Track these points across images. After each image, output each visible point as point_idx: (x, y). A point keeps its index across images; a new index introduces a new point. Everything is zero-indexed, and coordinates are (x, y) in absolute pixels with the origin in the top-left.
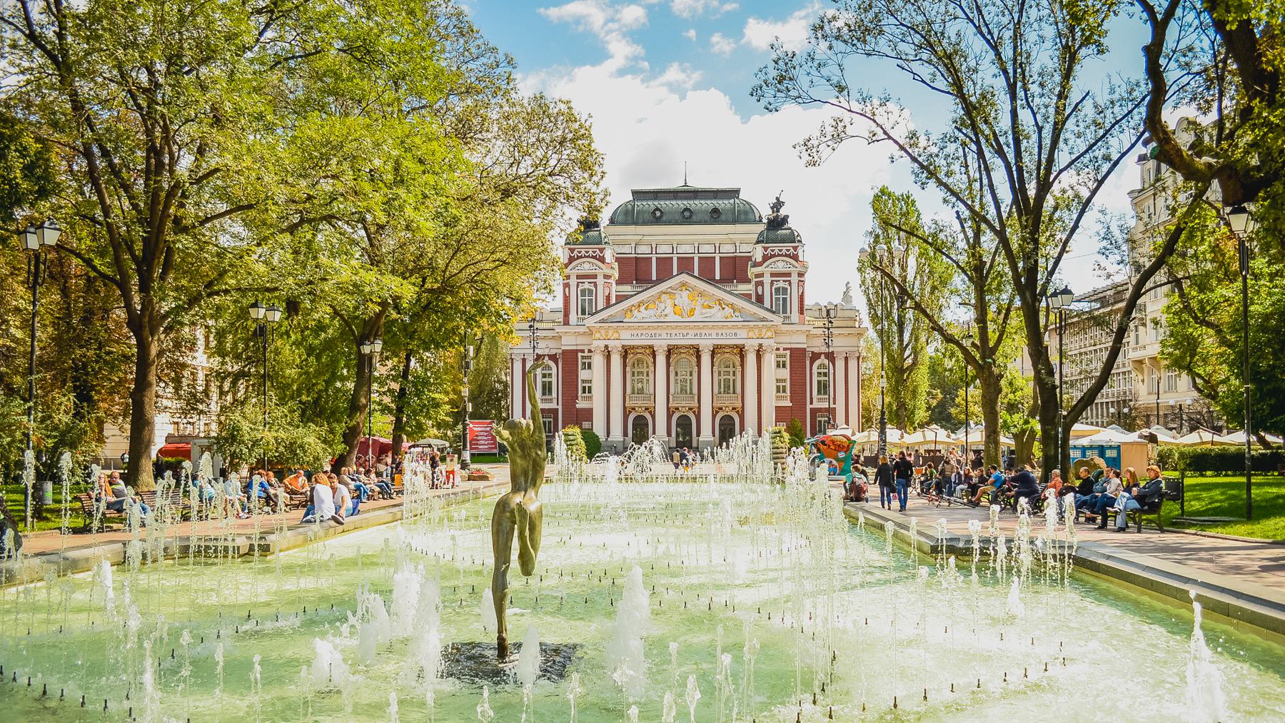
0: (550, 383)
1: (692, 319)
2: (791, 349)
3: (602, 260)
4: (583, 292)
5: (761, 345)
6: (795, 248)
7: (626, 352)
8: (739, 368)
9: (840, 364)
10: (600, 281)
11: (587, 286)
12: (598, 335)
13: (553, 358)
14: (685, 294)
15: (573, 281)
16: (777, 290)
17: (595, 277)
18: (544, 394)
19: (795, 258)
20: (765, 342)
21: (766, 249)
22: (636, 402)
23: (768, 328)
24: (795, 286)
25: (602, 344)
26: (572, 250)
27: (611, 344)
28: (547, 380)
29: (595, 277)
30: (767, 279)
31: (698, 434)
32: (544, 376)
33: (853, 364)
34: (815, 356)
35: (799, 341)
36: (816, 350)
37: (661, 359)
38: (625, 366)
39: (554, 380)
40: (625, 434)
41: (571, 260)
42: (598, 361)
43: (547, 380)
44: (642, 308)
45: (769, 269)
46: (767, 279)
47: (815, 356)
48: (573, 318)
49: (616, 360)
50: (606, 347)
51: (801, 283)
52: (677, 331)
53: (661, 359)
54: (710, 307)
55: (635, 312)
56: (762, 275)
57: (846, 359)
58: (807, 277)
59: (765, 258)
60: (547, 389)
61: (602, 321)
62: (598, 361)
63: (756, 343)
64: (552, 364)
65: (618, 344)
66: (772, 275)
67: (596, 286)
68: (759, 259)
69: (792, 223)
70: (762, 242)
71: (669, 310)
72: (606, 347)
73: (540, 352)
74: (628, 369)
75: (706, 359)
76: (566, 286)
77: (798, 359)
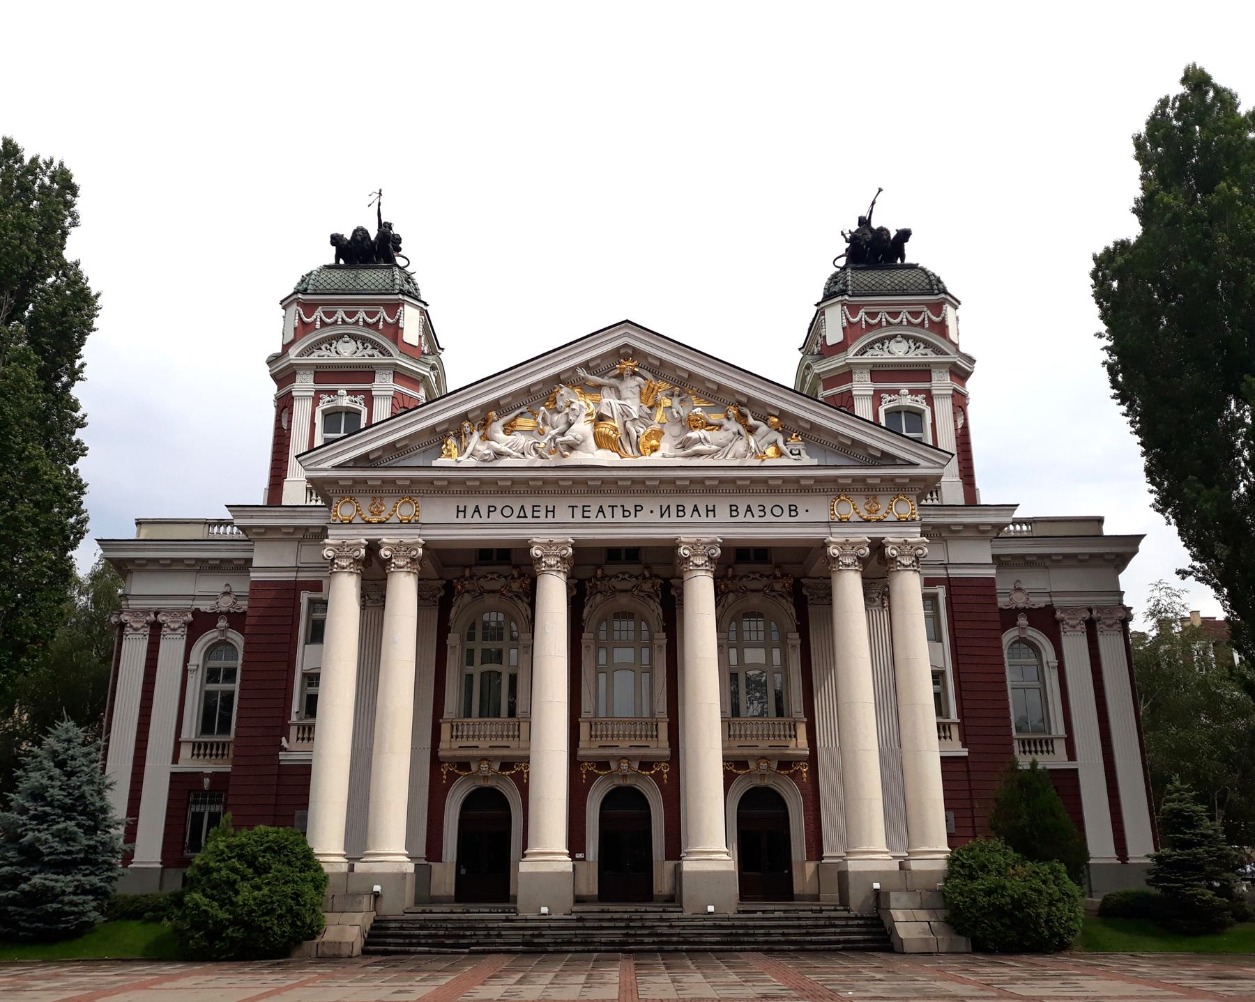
0: (228, 697)
1: (654, 459)
2: (949, 582)
3: (395, 332)
4: (332, 417)
5: (878, 546)
6: (937, 308)
7: (450, 589)
8: (795, 638)
9: (1075, 645)
10: (384, 385)
11: (345, 401)
12: (345, 511)
13: (237, 620)
14: (631, 386)
15: (304, 386)
16: (893, 414)
17: (366, 374)
18: (206, 727)
19: (941, 328)
20: (891, 536)
21: (854, 308)
22: (479, 739)
23: (897, 488)
24: (944, 408)
25: (361, 536)
26: (309, 308)
27: (388, 537)
28: (221, 687)
29: (366, 374)
30: (862, 386)
31: (675, 850)
32: (212, 676)
33: (1110, 646)
34: (1009, 618)
35: (974, 559)
36: (1002, 602)
37: (554, 594)
38: (443, 631)
39: (236, 687)
40: (434, 850)
41: (304, 328)
42: (345, 593)
43: (221, 687)
44: (497, 428)
45: (868, 358)
46: (862, 386)
47: (1009, 618)
48: (295, 491)
49: (404, 592)
50: (373, 547)
51: (960, 403)
52: (606, 502)
53: (554, 594)
54: (708, 425)
55: (474, 441)
56: (846, 375)
57: (1091, 629)
58: (971, 386)
59: (851, 331)
60: (214, 715)
61: (364, 461)
62: (345, 593)
63: (863, 535)
64: (237, 639)
65: (413, 536)
66: (879, 373)
67: (369, 400)
68: (834, 334)
69: (913, 253)
70: (843, 292)
71: (582, 428)
72: (373, 547)
73: (205, 606)
74: (453, 639)
75: (701, 593)
76: (284, 405)
77: (971, 619)
